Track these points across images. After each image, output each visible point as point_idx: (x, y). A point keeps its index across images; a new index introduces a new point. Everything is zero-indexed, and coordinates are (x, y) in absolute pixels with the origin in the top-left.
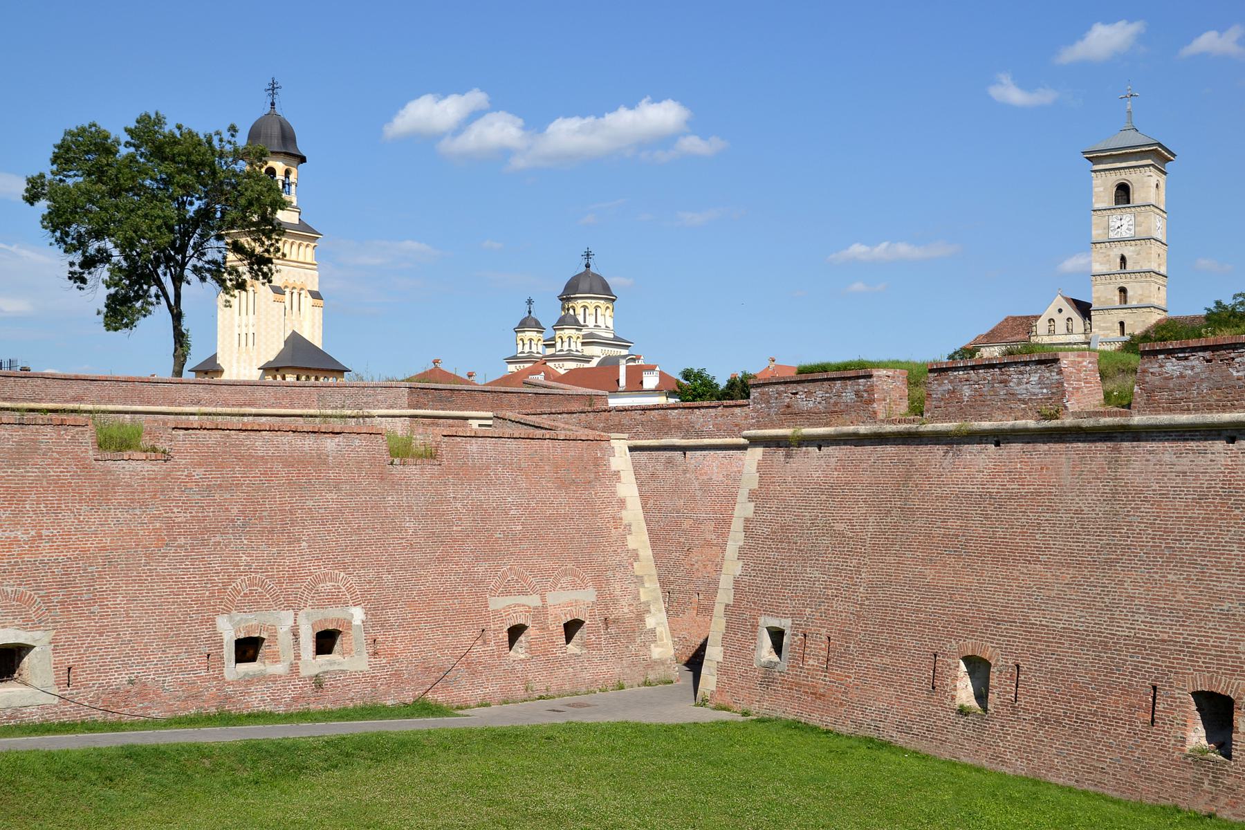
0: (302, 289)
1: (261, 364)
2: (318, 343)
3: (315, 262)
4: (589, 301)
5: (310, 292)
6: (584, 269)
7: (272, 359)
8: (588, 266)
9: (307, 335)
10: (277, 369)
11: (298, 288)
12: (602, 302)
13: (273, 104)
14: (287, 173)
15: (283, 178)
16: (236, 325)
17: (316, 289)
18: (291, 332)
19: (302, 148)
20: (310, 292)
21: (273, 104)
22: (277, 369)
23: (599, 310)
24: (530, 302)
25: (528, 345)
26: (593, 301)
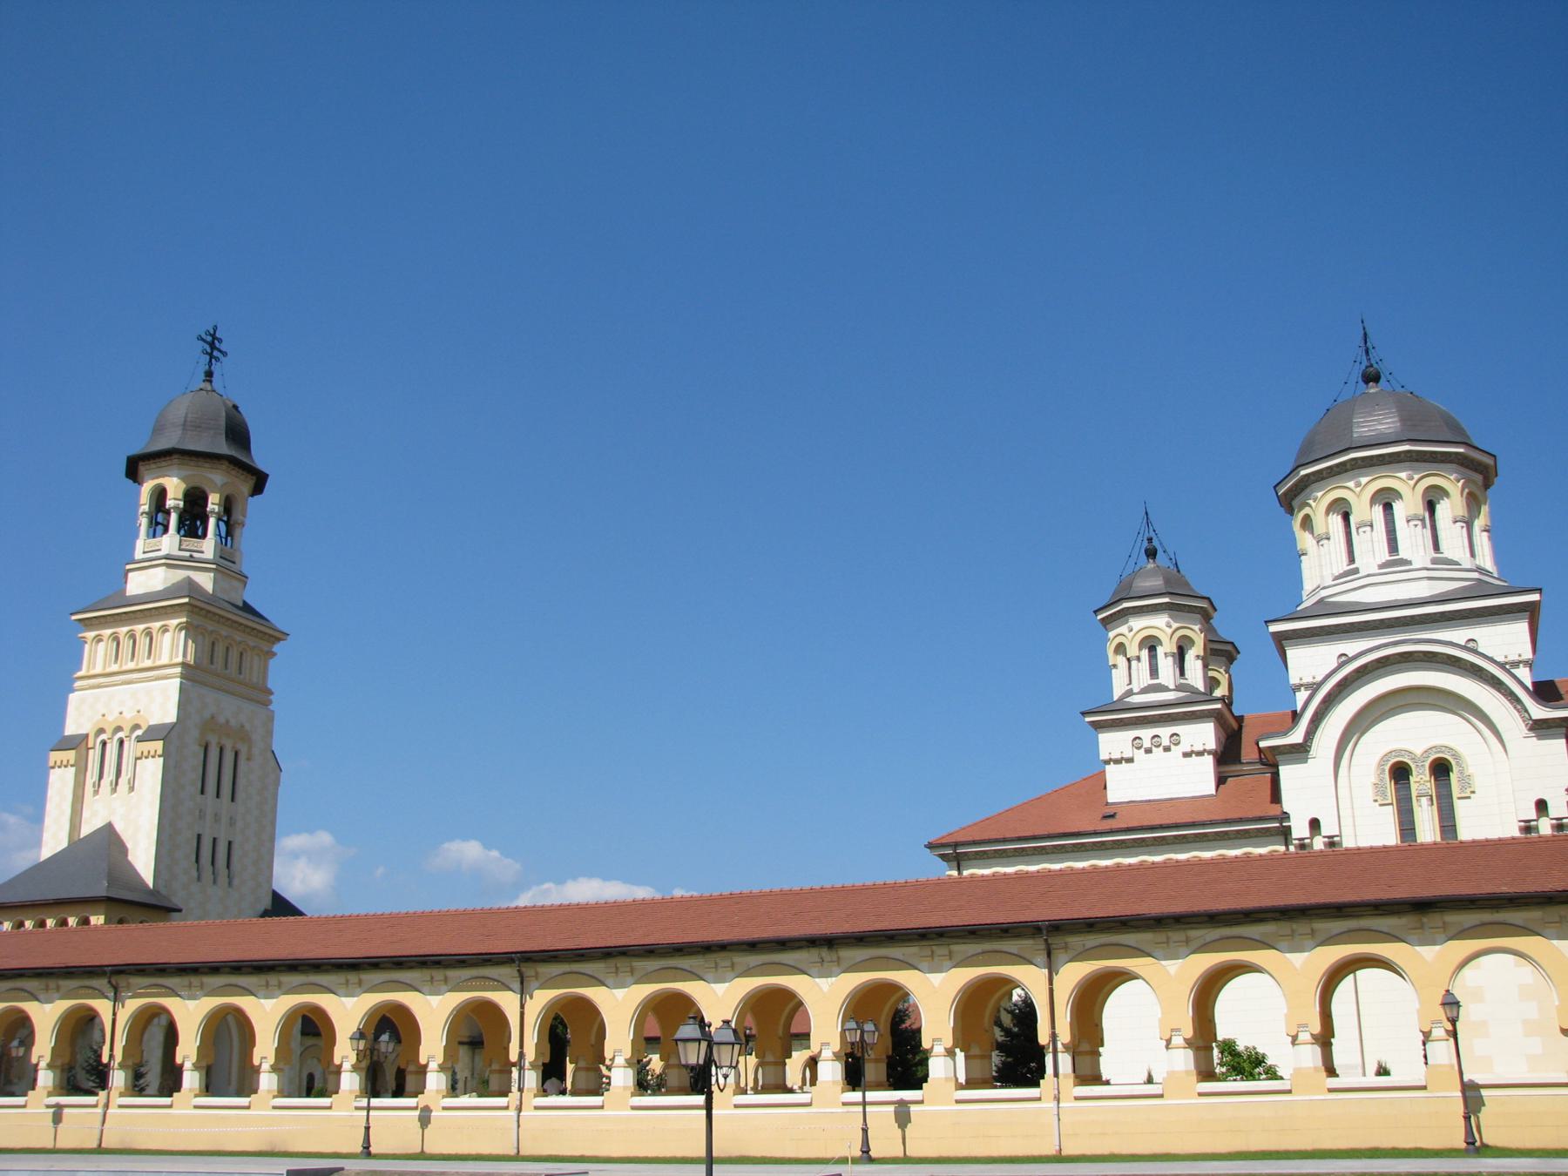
13: (209, 375)
19: (260, 456)
21: (209, 375)
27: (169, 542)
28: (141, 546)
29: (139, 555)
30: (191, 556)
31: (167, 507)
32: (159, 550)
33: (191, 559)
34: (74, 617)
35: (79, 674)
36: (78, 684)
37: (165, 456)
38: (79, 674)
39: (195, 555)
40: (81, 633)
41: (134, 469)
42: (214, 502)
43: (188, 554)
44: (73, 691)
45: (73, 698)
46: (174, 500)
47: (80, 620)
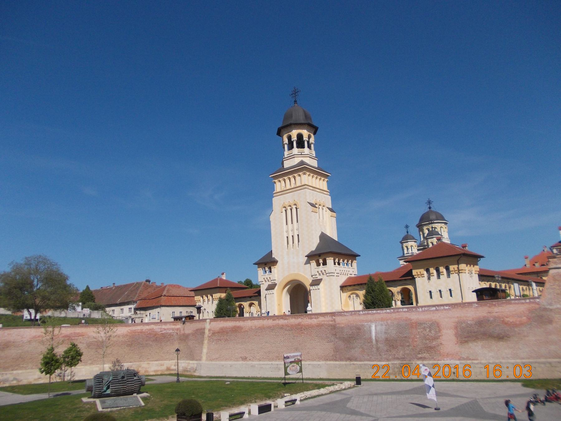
0: (324, 206)
1: (307, 254)
2: (337, 240)
3: (328, 191)
4: (437, 224)
5: (329, 209)
6: (428, 209)
7: (314, 249)
8: (430, 208)
9: (329, 234)
10: (320, 255)
11: (322, 205)
12: (443, 224)
14: (309, 137)
15: (307, 139)
16: (285, 231)
17: (330, 207)
18: (320, 233)
20: (329, 209)
22: (320, 255)
23: (442, 229)
24: (407, 227)
25: (411, 249)
26: (439, 224)
27: (295, 150)
28: (286, 153)
29: (286, 156)
30: (301, 154)
31: (292, 140)
32: (292, 153)
33: (301, 154)
34: (270, 176)
35: (274, 192)
36: (274, 195)
37: (286, 127)
38: (274, 192)
39: (302, 153)
40: (273, 180)
41: (279, 133)
42: (305, 138)
43: (300, 153)
44: (273, 197)
45: (274, 199)
46: (294, 138)
47: (272, 177)
